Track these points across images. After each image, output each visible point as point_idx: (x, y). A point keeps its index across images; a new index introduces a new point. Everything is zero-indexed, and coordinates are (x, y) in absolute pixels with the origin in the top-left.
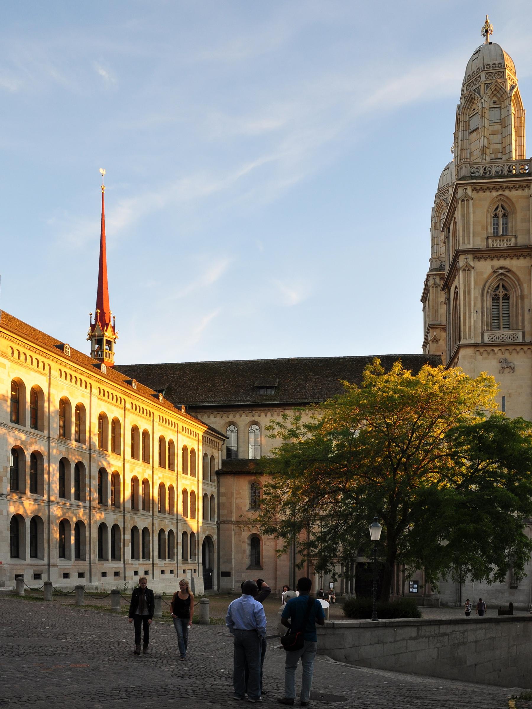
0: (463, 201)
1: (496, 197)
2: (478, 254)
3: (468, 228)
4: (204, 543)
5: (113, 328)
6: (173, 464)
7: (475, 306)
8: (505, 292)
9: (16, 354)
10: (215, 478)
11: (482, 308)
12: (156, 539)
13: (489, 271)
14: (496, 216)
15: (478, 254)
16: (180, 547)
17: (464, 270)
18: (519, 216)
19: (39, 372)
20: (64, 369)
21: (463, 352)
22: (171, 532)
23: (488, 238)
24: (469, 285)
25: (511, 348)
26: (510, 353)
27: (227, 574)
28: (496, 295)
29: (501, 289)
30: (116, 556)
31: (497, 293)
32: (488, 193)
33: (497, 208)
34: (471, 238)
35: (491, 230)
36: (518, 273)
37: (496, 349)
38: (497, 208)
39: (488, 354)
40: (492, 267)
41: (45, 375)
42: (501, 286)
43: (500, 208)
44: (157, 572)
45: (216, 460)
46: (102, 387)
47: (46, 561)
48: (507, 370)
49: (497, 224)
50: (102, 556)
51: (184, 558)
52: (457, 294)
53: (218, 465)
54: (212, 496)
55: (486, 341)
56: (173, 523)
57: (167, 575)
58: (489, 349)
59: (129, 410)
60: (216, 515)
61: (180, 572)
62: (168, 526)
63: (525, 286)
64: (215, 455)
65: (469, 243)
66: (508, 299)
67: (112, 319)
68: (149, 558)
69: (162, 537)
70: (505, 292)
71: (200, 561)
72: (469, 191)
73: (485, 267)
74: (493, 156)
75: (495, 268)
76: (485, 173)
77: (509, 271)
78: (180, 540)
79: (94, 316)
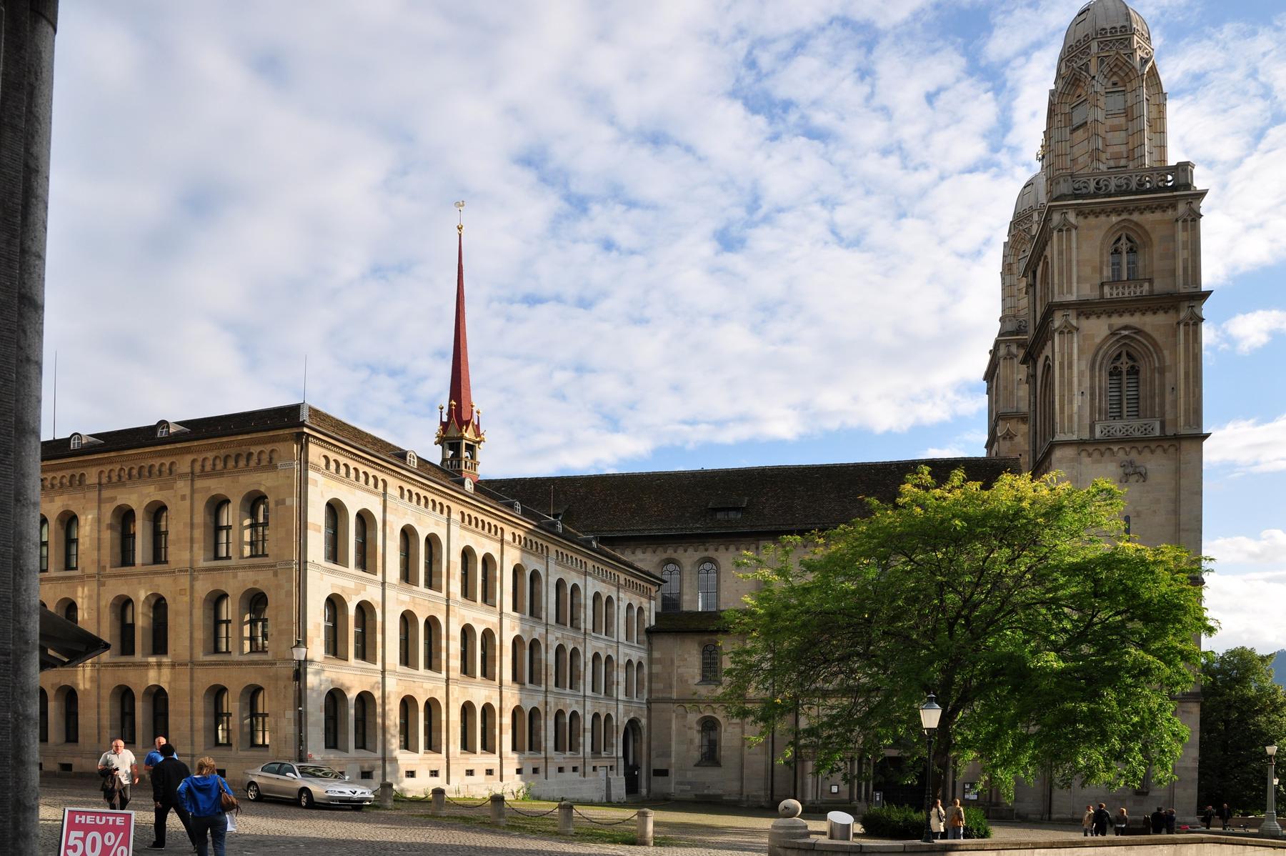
0: (1060, 230)
1: (1118, 223)
2: (1085, 308)
3: (1070, 270)
4: (626, 729)
5: (478, 426)
6: (579, 618)
7: (1080, 385)
8: (1131, 363)
9: (333, 466)
10: (643, 637)
11: (1092, 388)
12: (551, 723)
13: (1105, 332)
14: (1116, 252)
15: (1085, 308)
16: (588, 735)
17: (1061, 333)
18: (1157, 250)
19: (368, 491)
20: (406, 487)
21: (1058, 454)
22: (574, 714)
23: (1102, 285)
24: (1070, 355)
25: (1140, 446)
26: (1140, 453)
27: (664, 773)
28: (1115, 368)
29: (1124, 358)
30: (488, 747)
31: (1118, 364)
32: (1103, 218)
33: (1119, 239)
34: (1075, 285)
35: (1107, 272)
36: (1156, 335)
37: (1115, 448)
38: (1119, 239)
39: (1102, 454)
40: (1110, 326)
41: (377, 494)
42: (1124, 354)
43: (1124, 240)
44: (552, 770)
45: (646, 613)
46: (467, 511)
47: (379, 753)
48: (1133, 479)
49: (1119, 264)
50: (467, 746)
51: (595, 750)
52: (1048, 369)
53: (650, 620)
54: (640, 664)
55: (1098, 435)
56: (577, 702)
57: (569, 774)
58: (1103, 448)
59: (509, 543)
60: (645, 691)
61: (589, 769)
62: (571, 705)
63: (1166, 353)
64: (645, 605)
65: (1070, 292)
66: (1137, 373)
67: (475, 414)
68: (539, 750)
69: (561, 720)
70: (1131, 363)
71: (620, 754)
72: (1072, 217)
73: (1098, 328)
74: (1112, 163)
75: (1115, 328)
76: (1099, 189)
77: (1138, 331)
78: (588, 725)
79: (446, 410)
